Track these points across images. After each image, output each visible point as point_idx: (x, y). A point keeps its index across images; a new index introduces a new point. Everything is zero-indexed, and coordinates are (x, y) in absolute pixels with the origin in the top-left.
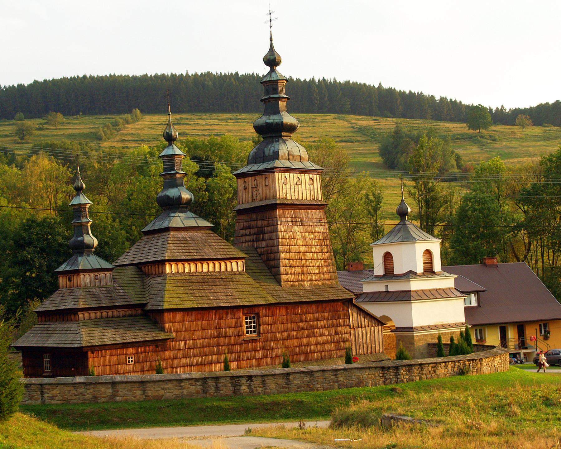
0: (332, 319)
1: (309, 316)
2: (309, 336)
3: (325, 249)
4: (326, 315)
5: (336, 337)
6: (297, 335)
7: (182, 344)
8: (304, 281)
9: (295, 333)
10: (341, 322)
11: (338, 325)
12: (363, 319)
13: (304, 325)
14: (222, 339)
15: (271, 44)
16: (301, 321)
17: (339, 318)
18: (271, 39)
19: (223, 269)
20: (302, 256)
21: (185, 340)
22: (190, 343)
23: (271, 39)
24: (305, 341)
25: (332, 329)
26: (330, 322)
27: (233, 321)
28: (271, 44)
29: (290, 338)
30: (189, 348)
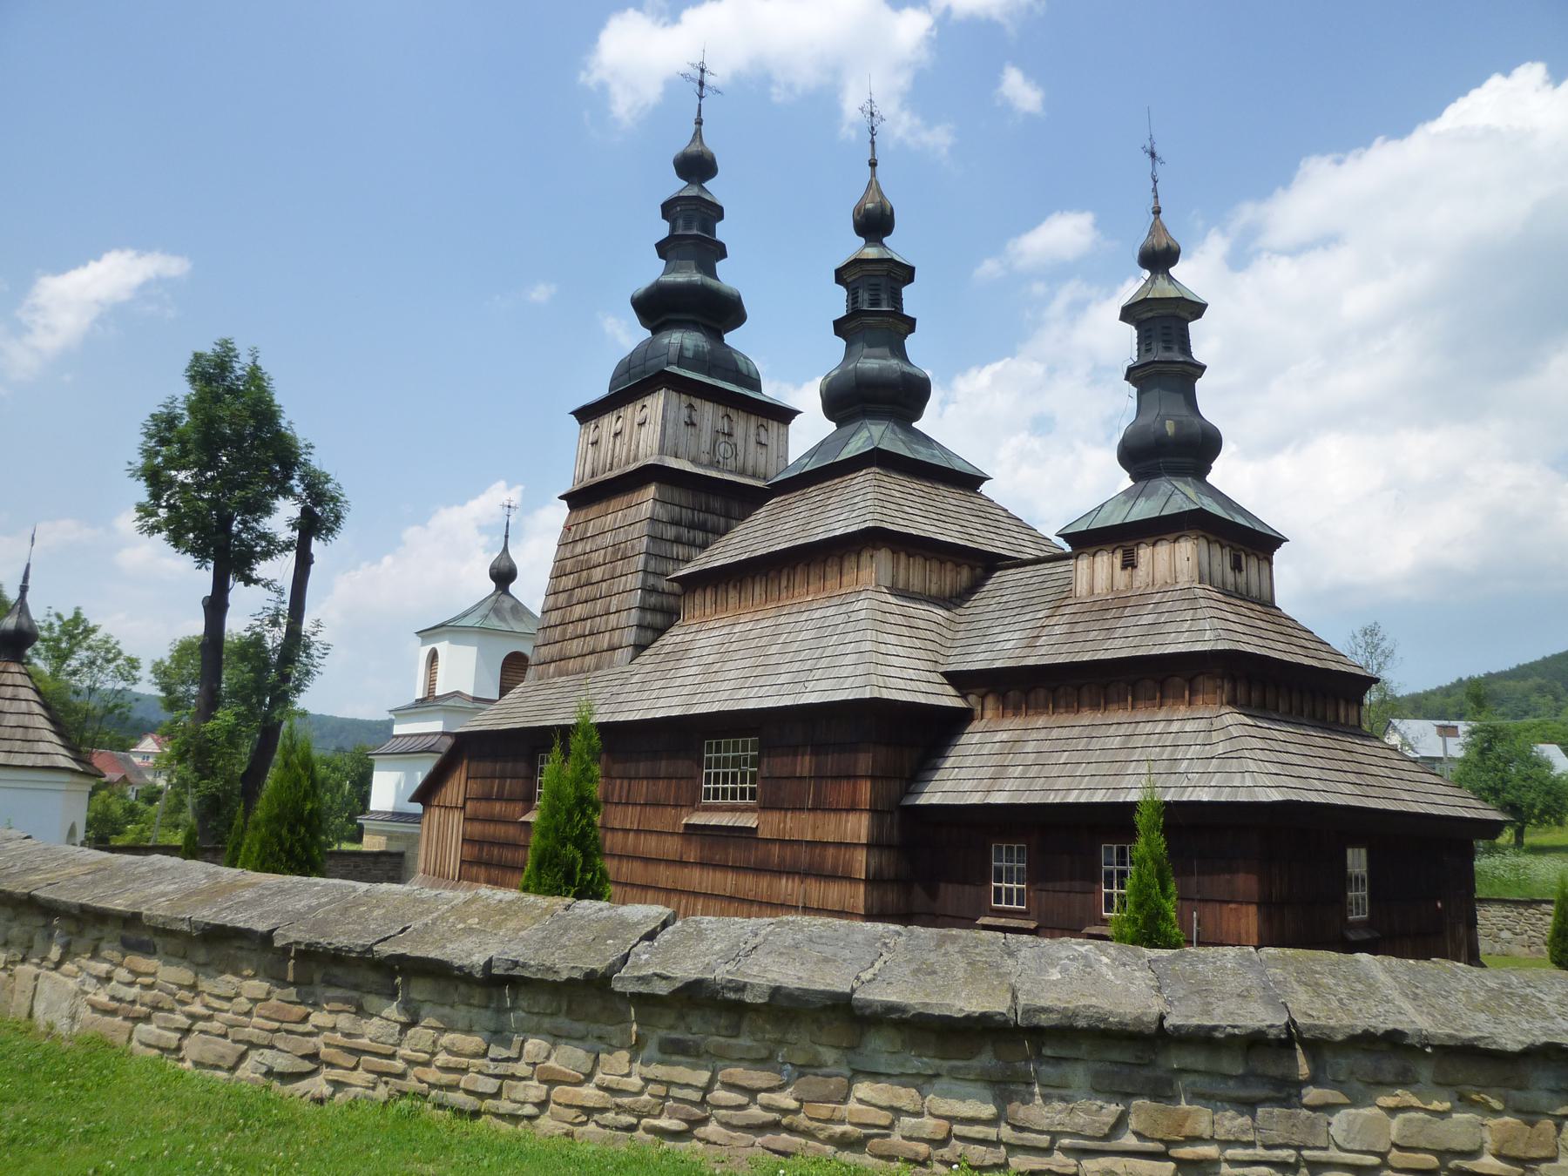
18: (699, 122)
23: (699, 122)
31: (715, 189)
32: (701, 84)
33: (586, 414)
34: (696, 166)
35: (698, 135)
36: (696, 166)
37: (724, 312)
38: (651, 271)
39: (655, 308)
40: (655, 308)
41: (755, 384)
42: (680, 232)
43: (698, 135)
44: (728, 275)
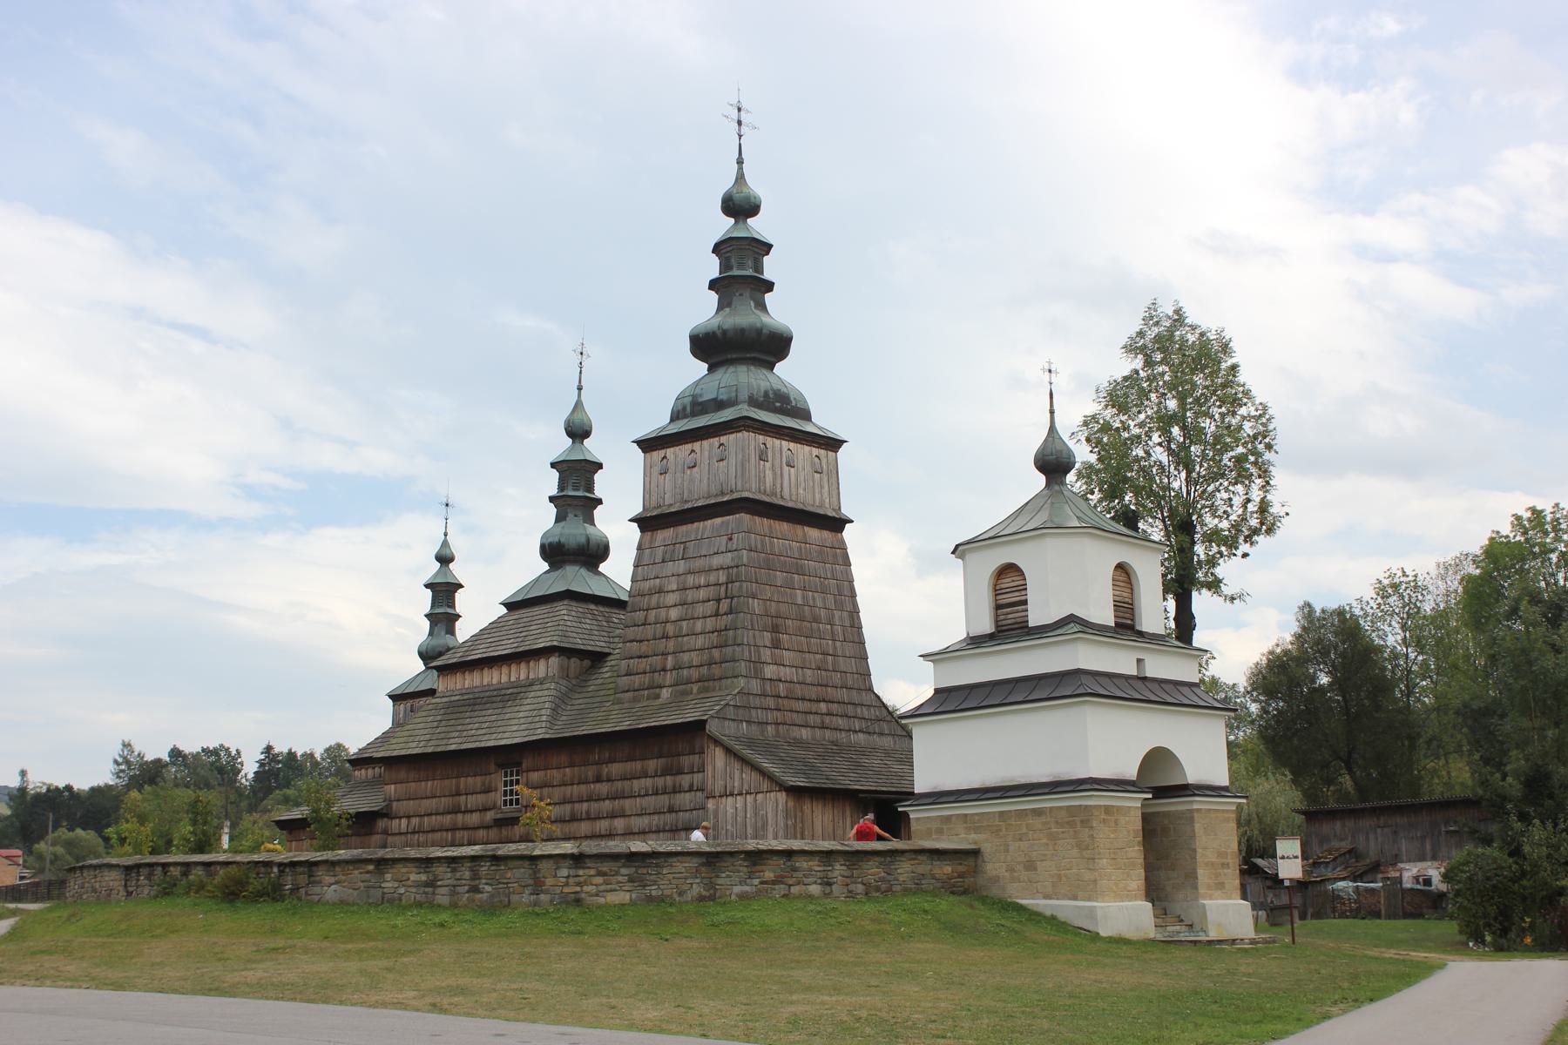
0: (663, 775)
1: (616, 769)
2: (612, 816)
3: (724, 605)
4: (652, 765)
5: (669, 818)
6: (588, 813)
7: (404, 821)
8: (661, 687)
9: (585, 805)
10: (685, 780)
11: (677, 790)
12: (737, 773)
13: (603, 788)
14: (460, 816)
15: (740, 169)
16: (598, 780)
17: (680, 772)
18: (740, 162)
19: (522, 677)
20: (670, 629)
21: (409, 817)
22: (415, 821)
23: (740, 162)
24: (603, 825)
25: (663, 800)
26: (660, 781)
27: (479, 779)
28: (740, 169)
29: (574, 819)
30: (414, 832)
31: (758, 226)
32: (740, 123)
33: (648, 445)
34: (739, 207)
35: (740, 177)
36: (739, 207)
37: (775, 346)
38: (704, 309)
39: (706, 345)
40: (710, 346)
41: (805, 415)
42: (736, 272)
43: (740, 177)
44: (779, 310)
